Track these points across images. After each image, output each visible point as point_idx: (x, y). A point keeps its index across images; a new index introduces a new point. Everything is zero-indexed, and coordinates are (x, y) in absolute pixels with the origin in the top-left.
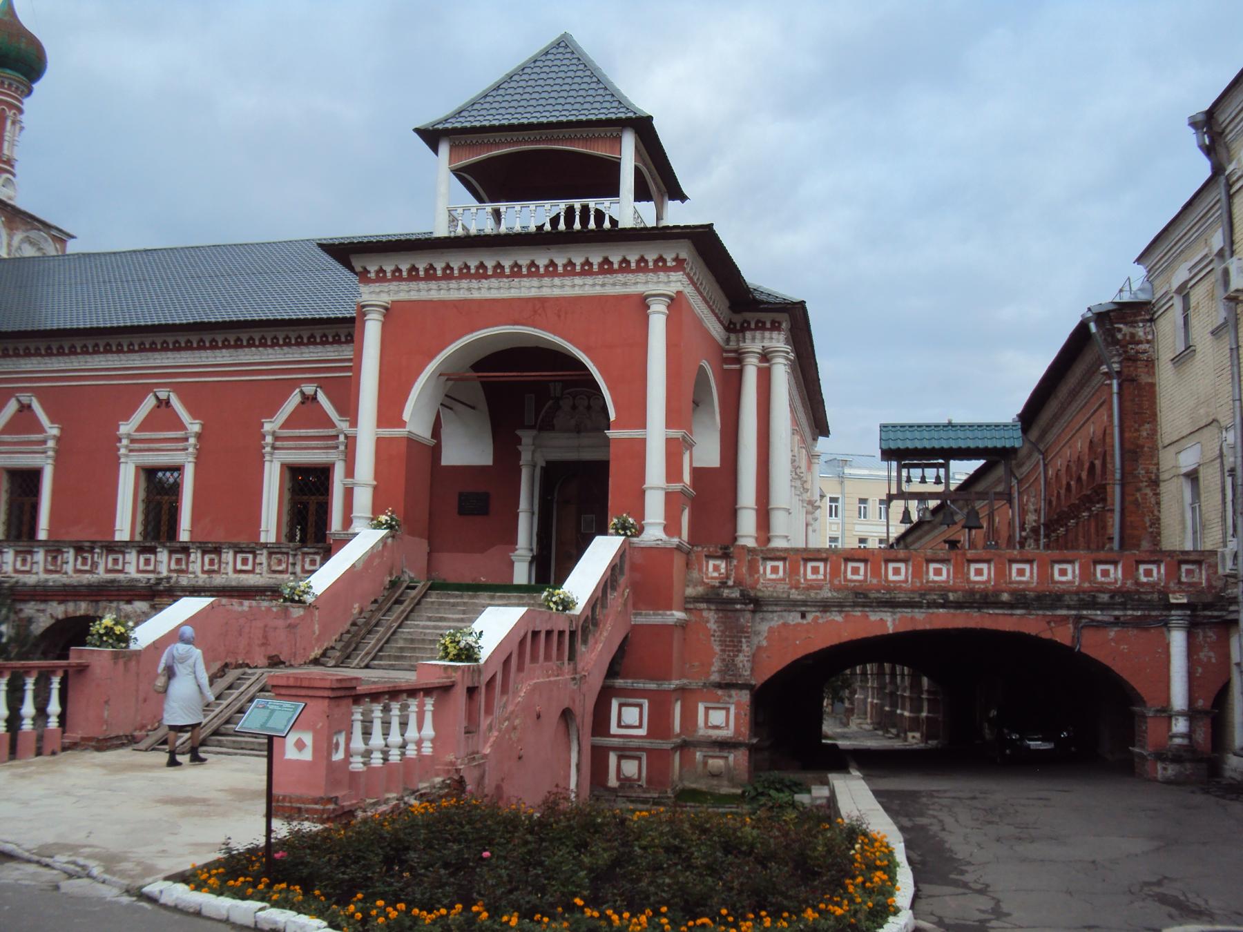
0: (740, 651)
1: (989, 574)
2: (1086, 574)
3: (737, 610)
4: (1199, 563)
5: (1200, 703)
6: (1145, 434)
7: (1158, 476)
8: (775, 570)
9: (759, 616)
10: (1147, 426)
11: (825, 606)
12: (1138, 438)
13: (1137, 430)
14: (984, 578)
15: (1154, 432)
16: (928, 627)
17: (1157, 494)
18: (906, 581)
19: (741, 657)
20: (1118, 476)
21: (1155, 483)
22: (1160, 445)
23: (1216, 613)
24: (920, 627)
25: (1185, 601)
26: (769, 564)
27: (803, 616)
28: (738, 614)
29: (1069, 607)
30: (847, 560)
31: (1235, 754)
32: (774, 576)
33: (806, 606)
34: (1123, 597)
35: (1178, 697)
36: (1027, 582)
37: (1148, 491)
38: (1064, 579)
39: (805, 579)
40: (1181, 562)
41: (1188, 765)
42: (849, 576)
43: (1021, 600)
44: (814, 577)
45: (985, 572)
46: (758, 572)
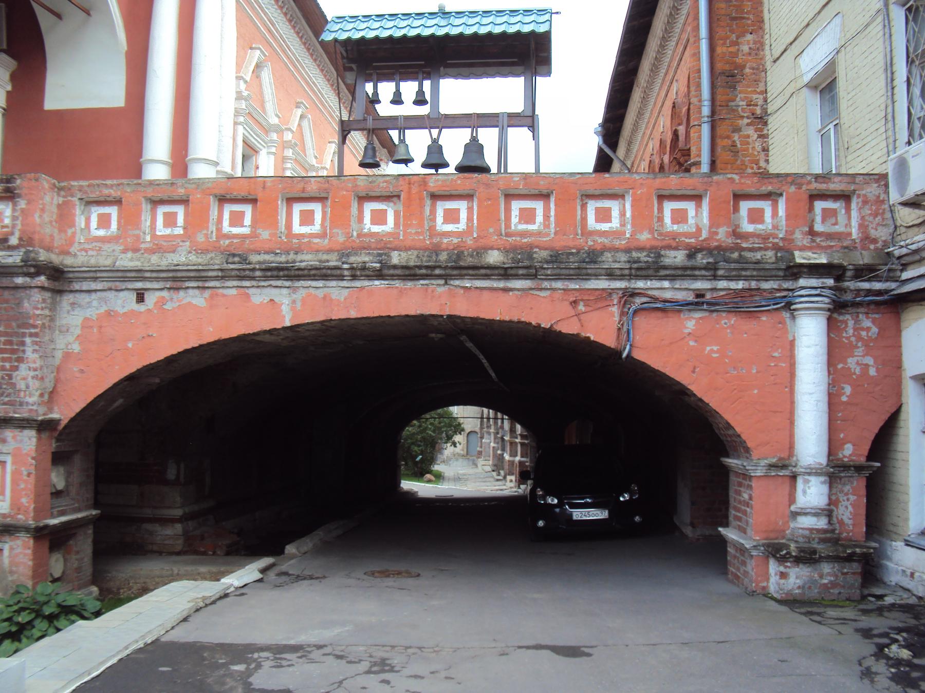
0: (20, 360)
1: (470, 219)
2: (641, 217)
3: (17, 288)
4: (845, 197)
5: (847, 451)
6: (745, 48)
7: (765, 111)
8: (104, 221)
9: (68, 299)
10: (749, 37)
11: (176, 279)
12: (736, 54)
13: (736, 43)
14: (462, 226)
15: (759, 46)
16: (353, 314)
17: (763, 137)
18: (323, 235)
19: (23, 370)
20: (706, 111)
21: (761, 120)
22: (769, 59)
23: (877, 286)
24: (338, 314)
25: (824, 260)
26: (95, 212)
27: (140, 298)
28: (21, 294)
29: (611, 275)
30: (223, 200)
31: (908, 544)
32: (101, 233)
33: (144, 279)
34: (710, 259)
35: (810, 440)
36: (539, 234)
37: (750, 131)
38: (605, 227)
39: (154, 236)
40: (815, 196)
41: (826, 568)
42: (226, 228)
43: (523, 265)
44: (168, 231)
45: (463, 215)
46: (72, 224)
